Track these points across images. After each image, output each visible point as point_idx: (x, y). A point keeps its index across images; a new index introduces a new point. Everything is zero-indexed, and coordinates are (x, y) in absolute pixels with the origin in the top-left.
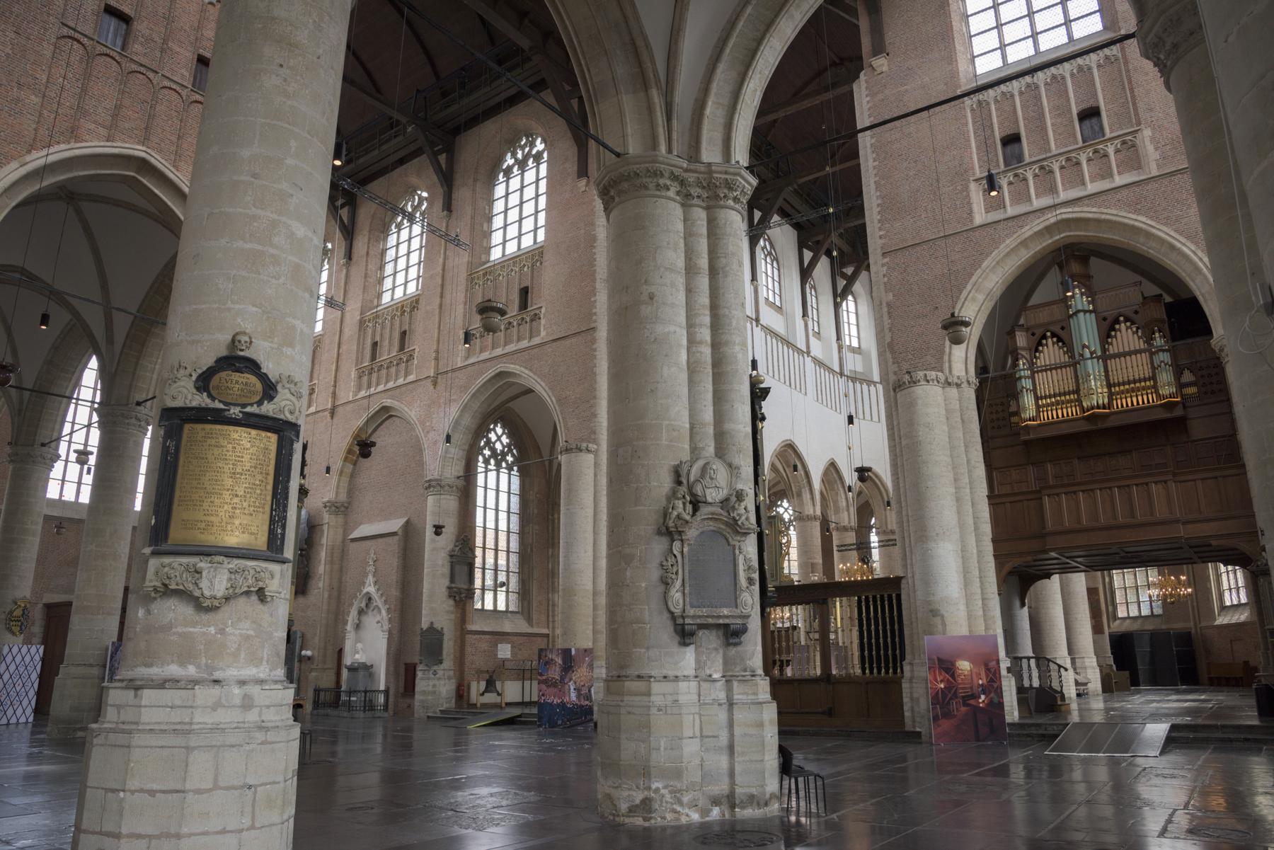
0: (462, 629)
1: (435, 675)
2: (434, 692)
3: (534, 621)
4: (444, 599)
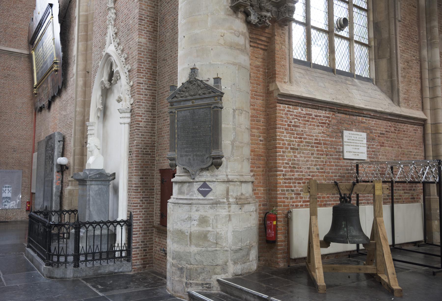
0: (268, 93)
1: (204, 194)
2: (204, 237)
3: (402, 95)
4: (222, 15)
